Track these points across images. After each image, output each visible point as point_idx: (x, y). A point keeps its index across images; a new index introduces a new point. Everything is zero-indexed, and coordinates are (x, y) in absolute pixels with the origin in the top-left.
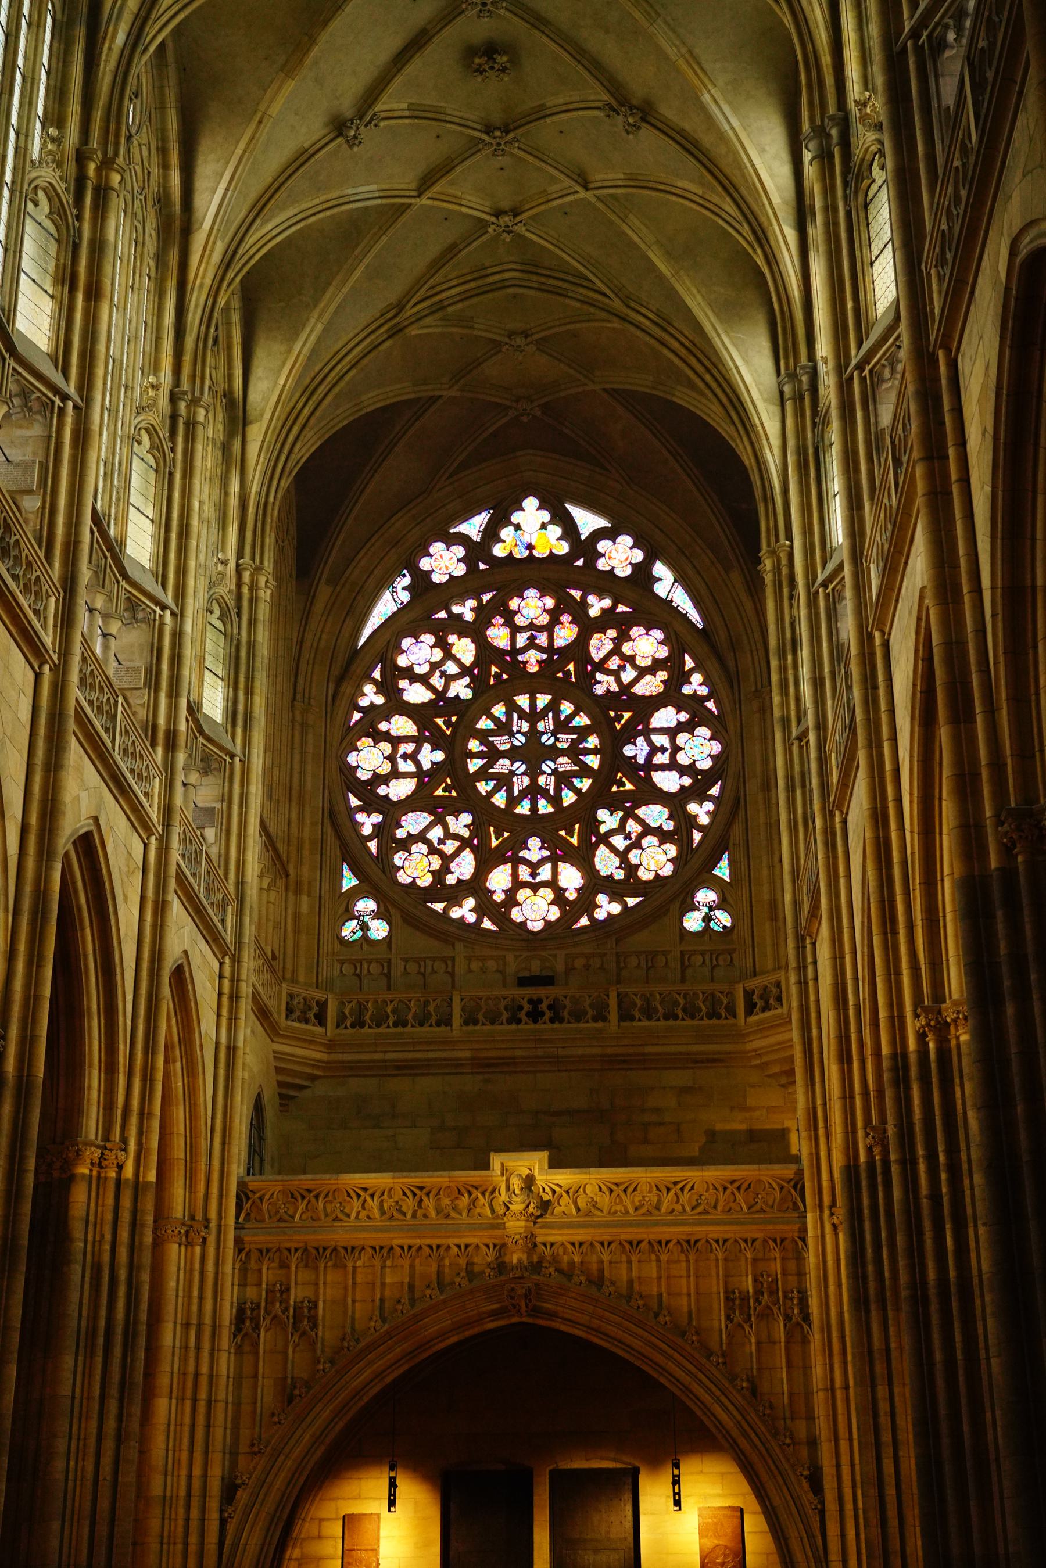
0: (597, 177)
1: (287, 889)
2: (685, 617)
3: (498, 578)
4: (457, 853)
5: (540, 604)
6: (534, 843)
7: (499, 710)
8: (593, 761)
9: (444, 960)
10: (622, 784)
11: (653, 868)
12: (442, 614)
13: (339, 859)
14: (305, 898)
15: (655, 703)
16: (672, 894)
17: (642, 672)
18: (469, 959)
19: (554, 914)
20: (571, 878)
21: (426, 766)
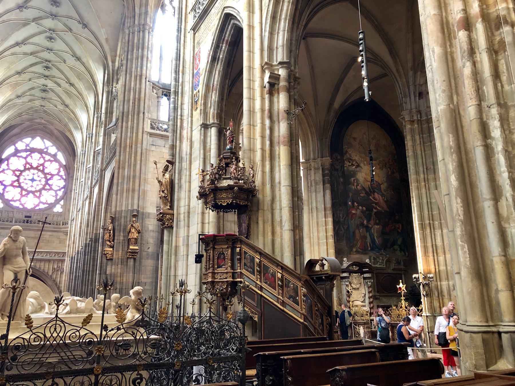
0: (59, 107)
16: (52, 206)
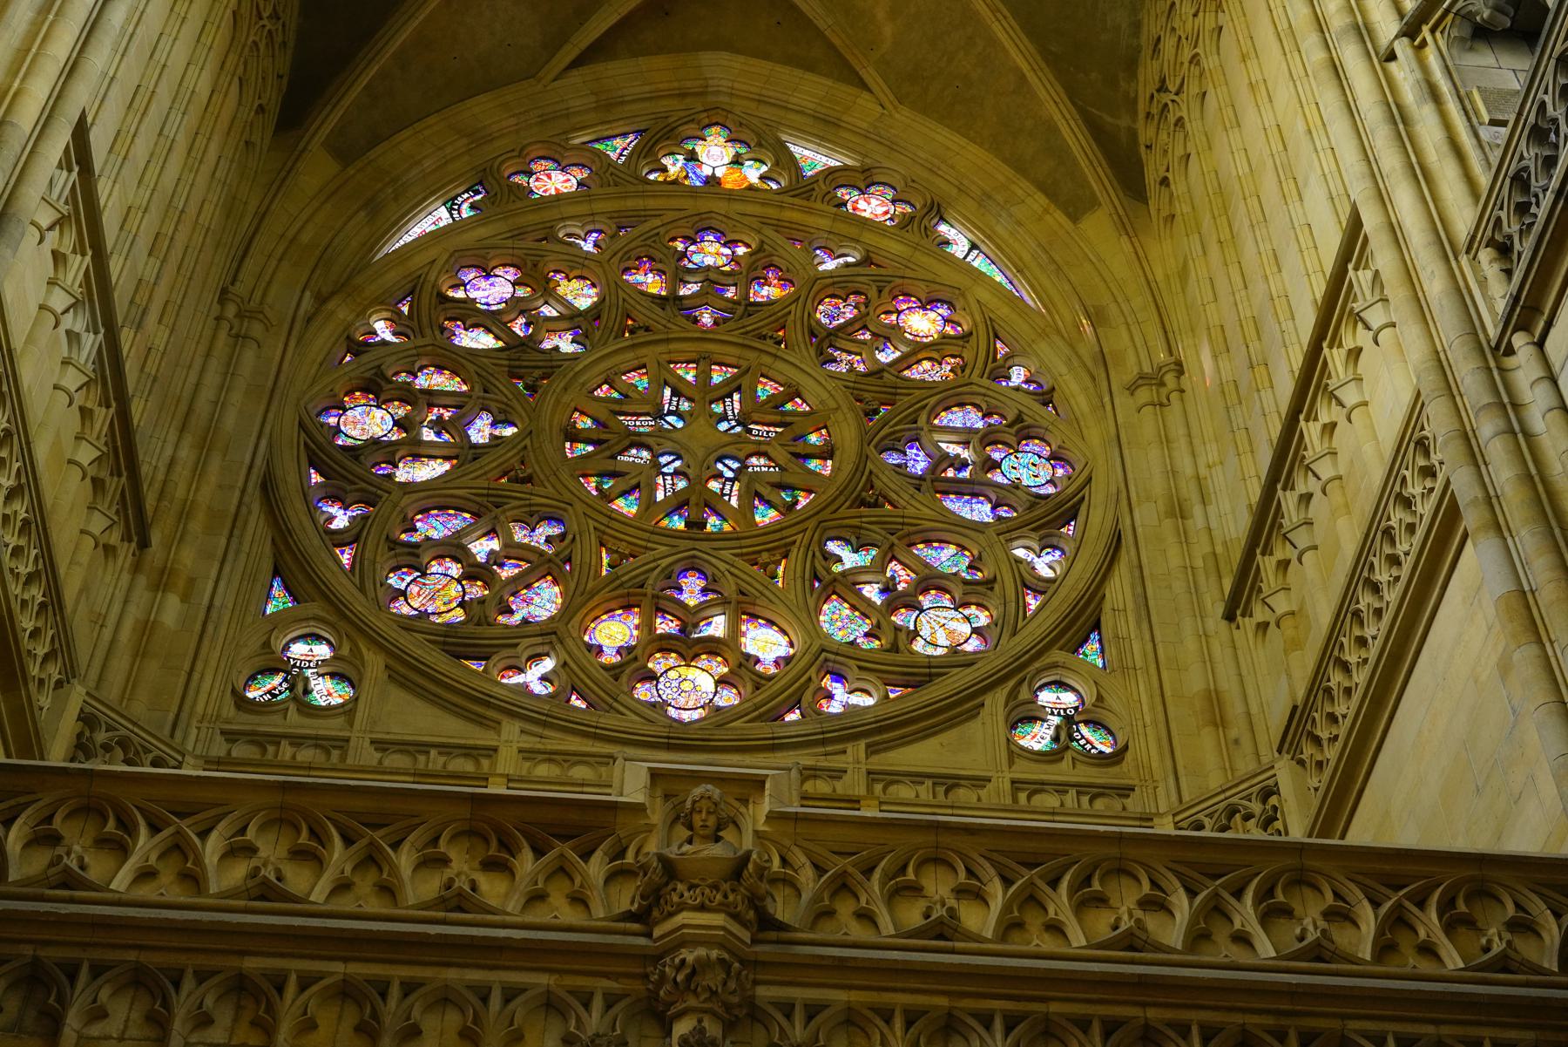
1: (136, 568)
4: (523, 583)
5: (728, 251)
9: (470, 751)
11: (942, 639)
13: (267, 565)
14: (173, 603)
18: (527, 754)
19: (728, 698)
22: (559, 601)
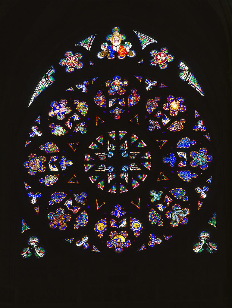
2: (194, 90)
3: (99, 70)
4: (79, 213)
5: (121, 83)
6: (118, 208)
7: (100, 140)
8: (148, 166)
10: (163, 177)
11: (178, 220)
12: (71, 89)
15: (179, 135)
17: (173, 119)
20: (136, 225)
21: (64, 167)
22: (88, 218)
